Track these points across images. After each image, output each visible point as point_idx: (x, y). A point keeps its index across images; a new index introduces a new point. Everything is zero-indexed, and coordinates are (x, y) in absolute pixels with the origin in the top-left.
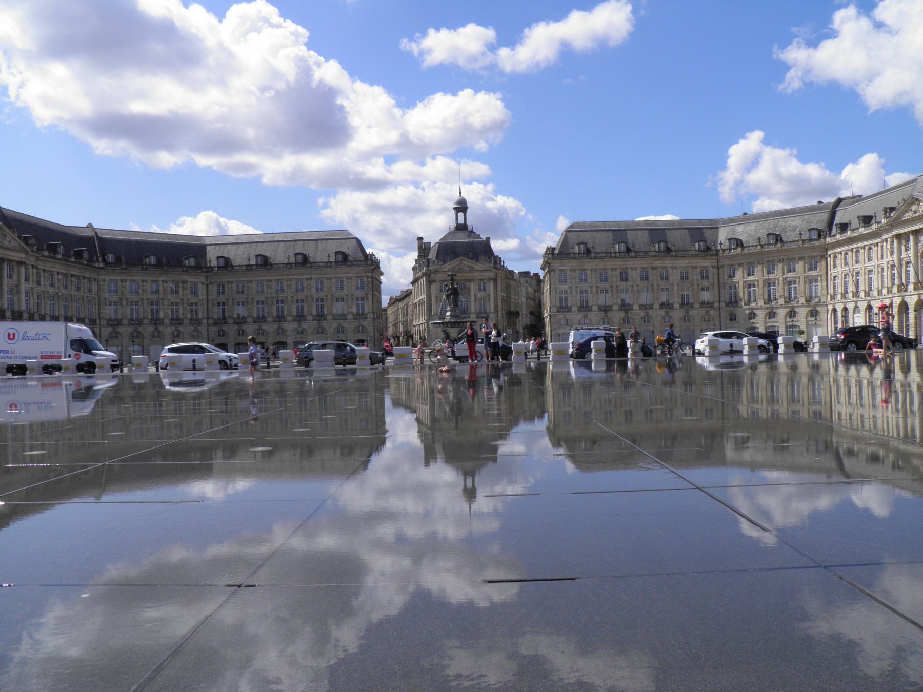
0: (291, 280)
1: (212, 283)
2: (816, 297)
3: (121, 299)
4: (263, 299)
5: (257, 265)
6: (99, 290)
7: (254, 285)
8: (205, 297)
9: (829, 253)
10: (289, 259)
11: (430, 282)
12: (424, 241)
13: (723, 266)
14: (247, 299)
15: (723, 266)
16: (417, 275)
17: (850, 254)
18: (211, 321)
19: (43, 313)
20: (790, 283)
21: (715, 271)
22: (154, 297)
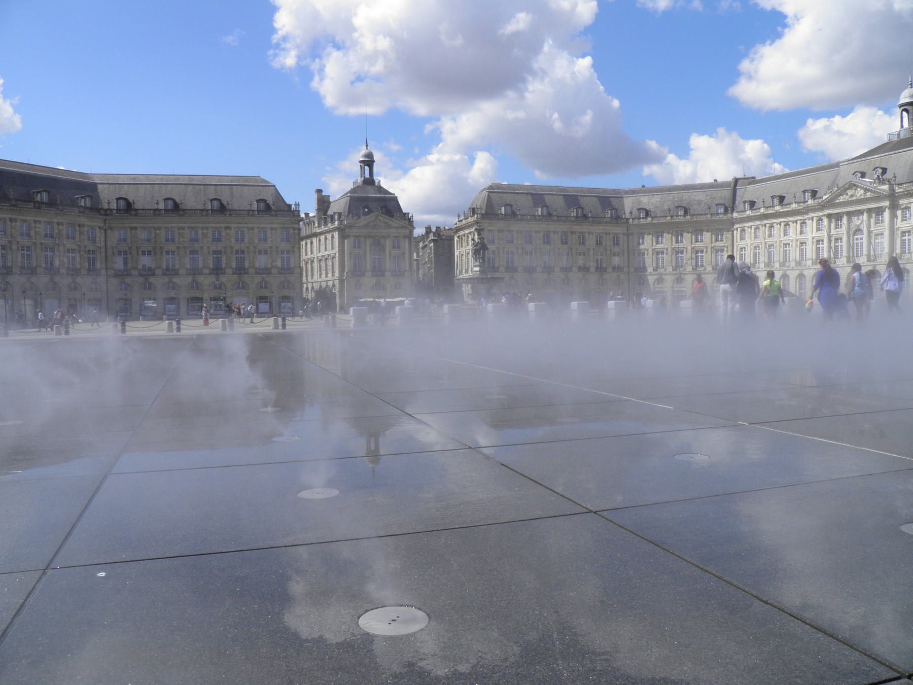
0: (207, 228)
1: (111, 228)
2: (702, 266)
3: (10, 242)
4: (174, 248)
5: (118, 210)
7: (163, 233)
8: (103, 244)
9: (736, 226)
10: (157, 203)
11: (342, 237)
12: (324, 194)
13: (633, 234)
14: (154, 248)
15: (633, 234)
17: (762, 229)
18: (111, 272)
20: (697, 252)
21: (626, 238)
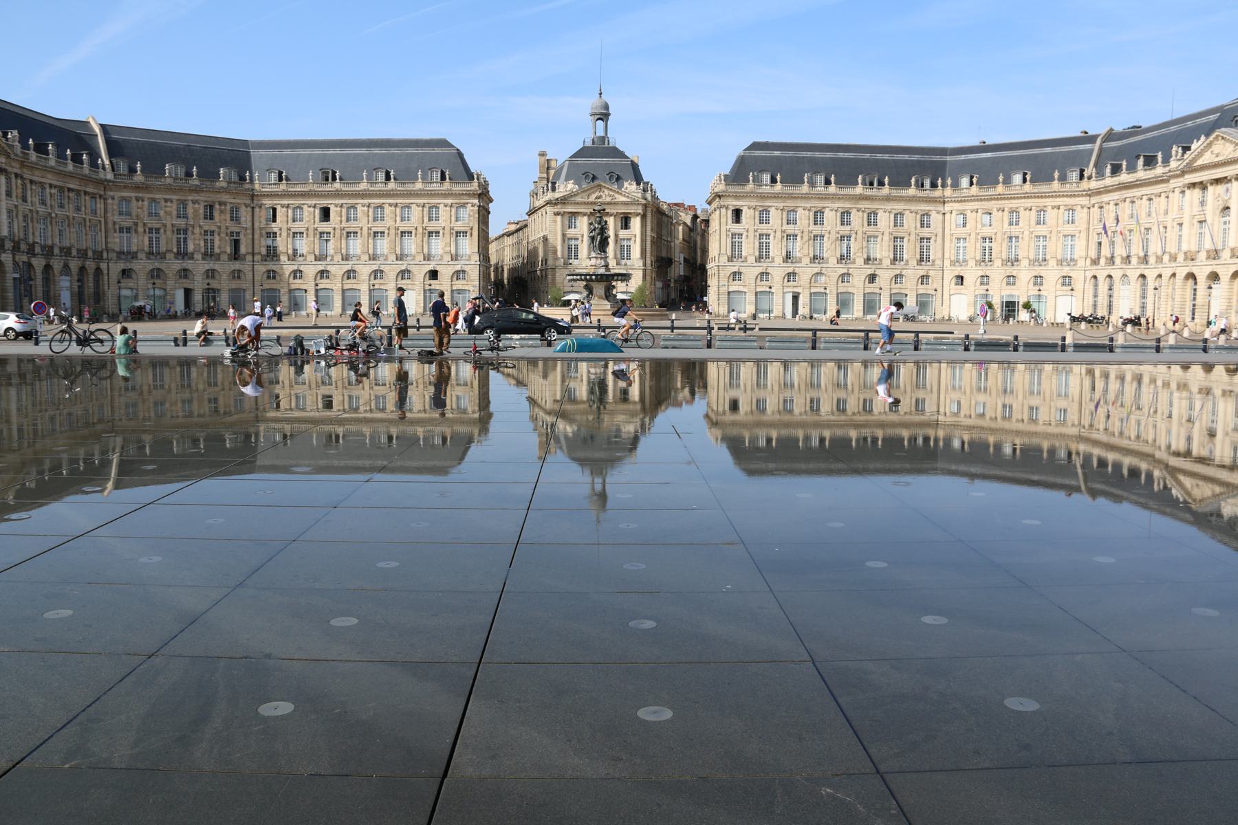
3: (136, 224)
6: (106, 211)
8: (249, 224)
16: (538, 204)
19: (31, 241)
21: (940, 217)
22: (181, 223)
